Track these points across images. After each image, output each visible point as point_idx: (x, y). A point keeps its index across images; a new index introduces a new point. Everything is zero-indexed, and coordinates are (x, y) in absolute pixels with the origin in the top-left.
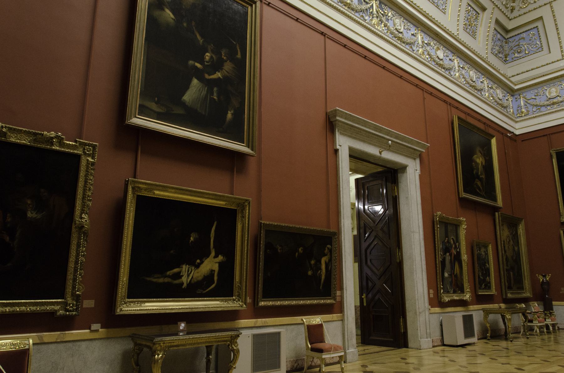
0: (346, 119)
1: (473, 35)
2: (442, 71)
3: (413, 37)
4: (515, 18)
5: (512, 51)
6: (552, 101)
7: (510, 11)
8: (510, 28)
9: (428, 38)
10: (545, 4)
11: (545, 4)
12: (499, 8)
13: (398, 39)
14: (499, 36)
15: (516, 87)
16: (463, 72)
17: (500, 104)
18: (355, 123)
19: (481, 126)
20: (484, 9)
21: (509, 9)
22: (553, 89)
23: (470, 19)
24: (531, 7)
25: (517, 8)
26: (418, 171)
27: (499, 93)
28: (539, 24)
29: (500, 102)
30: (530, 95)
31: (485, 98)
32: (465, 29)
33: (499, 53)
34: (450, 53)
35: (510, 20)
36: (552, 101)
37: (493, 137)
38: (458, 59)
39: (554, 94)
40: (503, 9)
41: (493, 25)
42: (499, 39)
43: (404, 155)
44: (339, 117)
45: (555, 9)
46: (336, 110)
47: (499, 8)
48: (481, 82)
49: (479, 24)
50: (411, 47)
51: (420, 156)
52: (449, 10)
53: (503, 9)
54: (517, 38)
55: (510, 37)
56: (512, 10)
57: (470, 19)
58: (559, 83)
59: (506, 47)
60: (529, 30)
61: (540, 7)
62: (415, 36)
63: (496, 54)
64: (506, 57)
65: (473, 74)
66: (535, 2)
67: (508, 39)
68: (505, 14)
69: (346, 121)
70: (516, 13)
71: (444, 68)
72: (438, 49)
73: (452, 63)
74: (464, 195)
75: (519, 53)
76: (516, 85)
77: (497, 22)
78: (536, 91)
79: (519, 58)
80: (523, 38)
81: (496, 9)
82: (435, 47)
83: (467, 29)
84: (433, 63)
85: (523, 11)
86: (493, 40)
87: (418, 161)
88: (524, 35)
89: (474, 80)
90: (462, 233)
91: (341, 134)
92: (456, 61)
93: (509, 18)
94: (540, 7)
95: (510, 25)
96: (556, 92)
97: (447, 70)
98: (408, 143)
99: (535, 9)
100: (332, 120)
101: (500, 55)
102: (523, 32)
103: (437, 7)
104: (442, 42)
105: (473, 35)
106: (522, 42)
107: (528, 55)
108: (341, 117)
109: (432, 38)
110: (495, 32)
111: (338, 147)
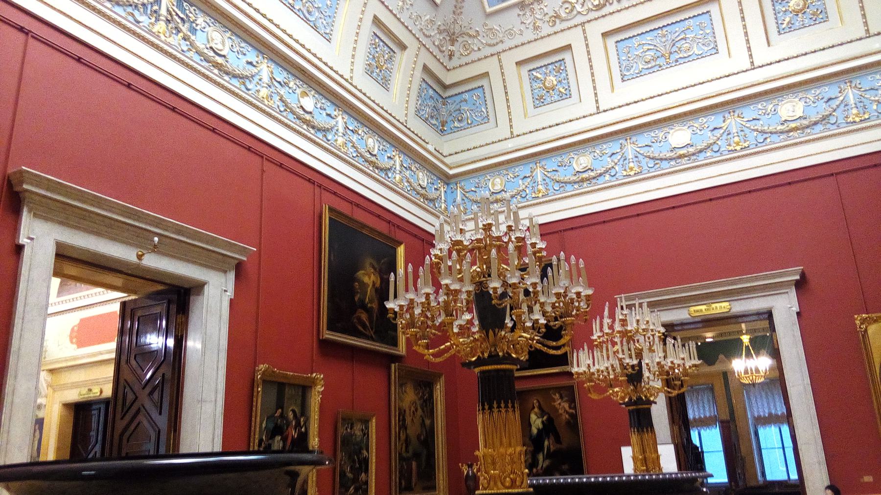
0: (47, 190)
1: (385, 84)
2: (311, 133)
3: (250, 67)
4: (454, 68)
5: (451, 118)
6: (494, 197)
7: (447, 58)
8: (448, 82)
9: (285, 74)
10: (492, 55)
11: (492, 55)
12: (428, 49)
13: (216, 67)
14: (431, 92)
15: (451, 172)
16: (355, 138)
17: (421, 195)
18: (75, 200)
19: (382, 227)
20: (403, 47)
21: (446, 53)
22: (498, 180)
23: (378, 57)
24: (475, 56)
25: (457, 54)
26: (230, 294)
27: (423, 178)
28: (484, 82)
29: (423, 192)
30: (469, 184)
31: (394, 184)
32: (369, 72)
33: (432, 117)
34: (329, 104)
35: (448, 70)
36: (494, 197)
37: (401, 244)
38: (346, 117)
39: (498, 187)
40: (436, 52)
41: (419, 74)
42: (431, 97)
43: (201, 265)
44: (27, 183)
45: (504, 63)
46: (21, 172)
47: (428, 49)
48: (389, 158)
49: (395, 67)
50: (244, 84)
51: (239, 268)
52: (337, 36)
53: (436, 52)
54: (458, 99)
55: (449, 97)
56: (451, 56)
57: (378, 57)
58: (505, 172)
59: (444, 111)
60: (472, 89)
61: (486, 57)
62: (254, 66)
63: (427, 119)
64: (443, 126)
65: (373, 143)
66: (479, 49)
67: (447, 99)
68: (439, 60)
69: (49, 194)
70: (455, 62)
71: (313, 127)
72: (305, 94)
73: (333, 122)
74: (328, 335)
75: (459, 121)
76: (451, 168)
77: (425, 68)
78: (477, 181)
79: (460, 129)
80: (466, 101)
81: (422, 48)
82: (298, 91)
83: (372, 72)
84: (291, 116)
85: (464, 60)
86: (420, 96)
87: (232, 276)
88: (466, 96)
89: (375, 153)
90: (315, 400)
91: (30, 211)
92: (340, 119)
93: (446, 67)
94: (486, 57)
95: (448, 79)
96: (501, 184)
97: (319, 130)
98: (207, 243)
99: (479, 60)
100: (17, 189)
101: (434, 122)
102: (466, 92)
103: (315, 28)
104: (313, 85)
105: (385, 84)
106: (465, 107)
107: (470, 125)
108: (32, 184)
109: (293, 75)
110: (424, 85)
111: (23, 240)
